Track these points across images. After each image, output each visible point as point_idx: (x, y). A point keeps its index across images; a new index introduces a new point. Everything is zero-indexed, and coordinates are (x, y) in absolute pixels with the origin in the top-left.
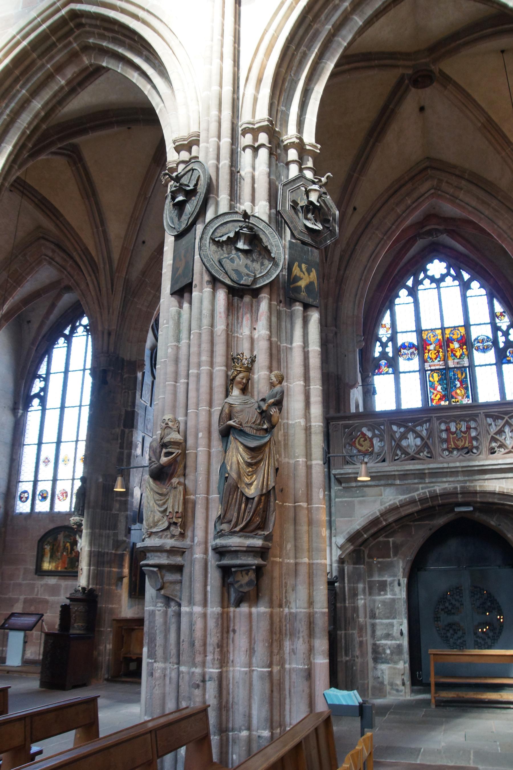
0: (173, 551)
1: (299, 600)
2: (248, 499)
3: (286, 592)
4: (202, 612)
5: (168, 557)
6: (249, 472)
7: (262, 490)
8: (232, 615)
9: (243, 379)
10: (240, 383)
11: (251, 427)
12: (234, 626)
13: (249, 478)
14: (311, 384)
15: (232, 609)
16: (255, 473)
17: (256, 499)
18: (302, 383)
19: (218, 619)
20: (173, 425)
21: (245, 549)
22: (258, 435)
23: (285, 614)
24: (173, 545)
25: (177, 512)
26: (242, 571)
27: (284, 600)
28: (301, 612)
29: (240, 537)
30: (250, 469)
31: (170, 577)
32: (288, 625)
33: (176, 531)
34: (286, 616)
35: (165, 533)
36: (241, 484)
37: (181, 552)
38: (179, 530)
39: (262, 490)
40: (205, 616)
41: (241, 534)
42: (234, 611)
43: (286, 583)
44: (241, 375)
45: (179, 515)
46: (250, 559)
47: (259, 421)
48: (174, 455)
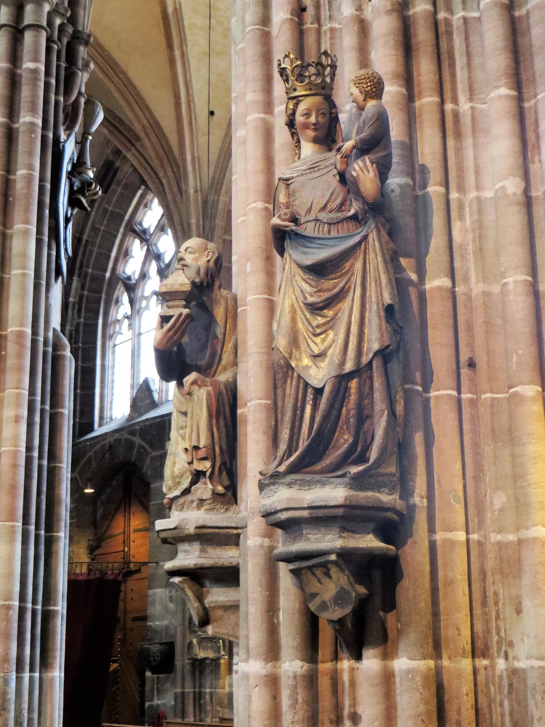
0: (206, 537)
1: (528, 636)
2: (319, 392)
3: (497, 618)
4: (264, 672)
5: (203, 551)
6: (318, 326)
7: (343, 363)
8: (346, 677)
9: (307, 115)
10: (306, 126)
11: (317, 220)
12: (354, 705)
13: (318, 340)
14: (538, 90)
15: (345, 664)
16: (331, 328)
17: (327, 390)
18: (504, 91)
19: (295, 687)
20: (196, 259)
21: (305, 514)
22: (334, 234)
23: (498, 673)
24: (201, 523)
25: (196, 448)
26: (310, 568)
27: (496, 638)
28: (532, 667)
29: (290, 485)
30: (321, 320)
31: (217, 595)
32: (506, 703)
33: (205, 489)
34: (501, 677)
35: (189, 498)
36: (299, 360)
37: (230, 538)
38: (210, 486)
39: (343, 363)
40: (273, 682)
41: (294, 477)
42: (352, 670)
43: (496, 594)
44: (302, 107)
45: (202, 453)
46: (329, 537)
47: (338, 201)
48: (173, 320)
